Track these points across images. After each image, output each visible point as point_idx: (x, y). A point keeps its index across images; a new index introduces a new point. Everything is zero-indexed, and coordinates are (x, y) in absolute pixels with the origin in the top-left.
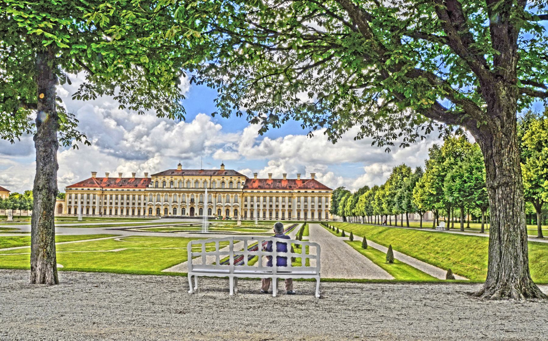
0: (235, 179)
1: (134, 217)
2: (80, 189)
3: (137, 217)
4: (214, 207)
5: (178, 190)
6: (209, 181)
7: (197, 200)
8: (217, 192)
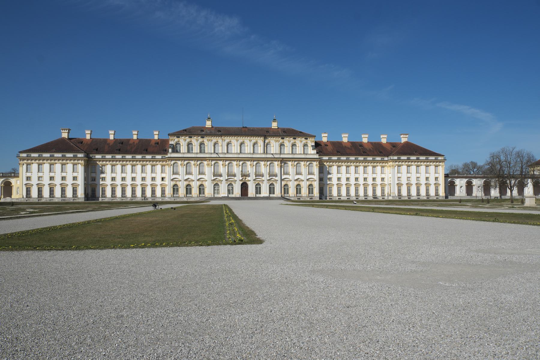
0: (300, 142)
5: (221, 156)
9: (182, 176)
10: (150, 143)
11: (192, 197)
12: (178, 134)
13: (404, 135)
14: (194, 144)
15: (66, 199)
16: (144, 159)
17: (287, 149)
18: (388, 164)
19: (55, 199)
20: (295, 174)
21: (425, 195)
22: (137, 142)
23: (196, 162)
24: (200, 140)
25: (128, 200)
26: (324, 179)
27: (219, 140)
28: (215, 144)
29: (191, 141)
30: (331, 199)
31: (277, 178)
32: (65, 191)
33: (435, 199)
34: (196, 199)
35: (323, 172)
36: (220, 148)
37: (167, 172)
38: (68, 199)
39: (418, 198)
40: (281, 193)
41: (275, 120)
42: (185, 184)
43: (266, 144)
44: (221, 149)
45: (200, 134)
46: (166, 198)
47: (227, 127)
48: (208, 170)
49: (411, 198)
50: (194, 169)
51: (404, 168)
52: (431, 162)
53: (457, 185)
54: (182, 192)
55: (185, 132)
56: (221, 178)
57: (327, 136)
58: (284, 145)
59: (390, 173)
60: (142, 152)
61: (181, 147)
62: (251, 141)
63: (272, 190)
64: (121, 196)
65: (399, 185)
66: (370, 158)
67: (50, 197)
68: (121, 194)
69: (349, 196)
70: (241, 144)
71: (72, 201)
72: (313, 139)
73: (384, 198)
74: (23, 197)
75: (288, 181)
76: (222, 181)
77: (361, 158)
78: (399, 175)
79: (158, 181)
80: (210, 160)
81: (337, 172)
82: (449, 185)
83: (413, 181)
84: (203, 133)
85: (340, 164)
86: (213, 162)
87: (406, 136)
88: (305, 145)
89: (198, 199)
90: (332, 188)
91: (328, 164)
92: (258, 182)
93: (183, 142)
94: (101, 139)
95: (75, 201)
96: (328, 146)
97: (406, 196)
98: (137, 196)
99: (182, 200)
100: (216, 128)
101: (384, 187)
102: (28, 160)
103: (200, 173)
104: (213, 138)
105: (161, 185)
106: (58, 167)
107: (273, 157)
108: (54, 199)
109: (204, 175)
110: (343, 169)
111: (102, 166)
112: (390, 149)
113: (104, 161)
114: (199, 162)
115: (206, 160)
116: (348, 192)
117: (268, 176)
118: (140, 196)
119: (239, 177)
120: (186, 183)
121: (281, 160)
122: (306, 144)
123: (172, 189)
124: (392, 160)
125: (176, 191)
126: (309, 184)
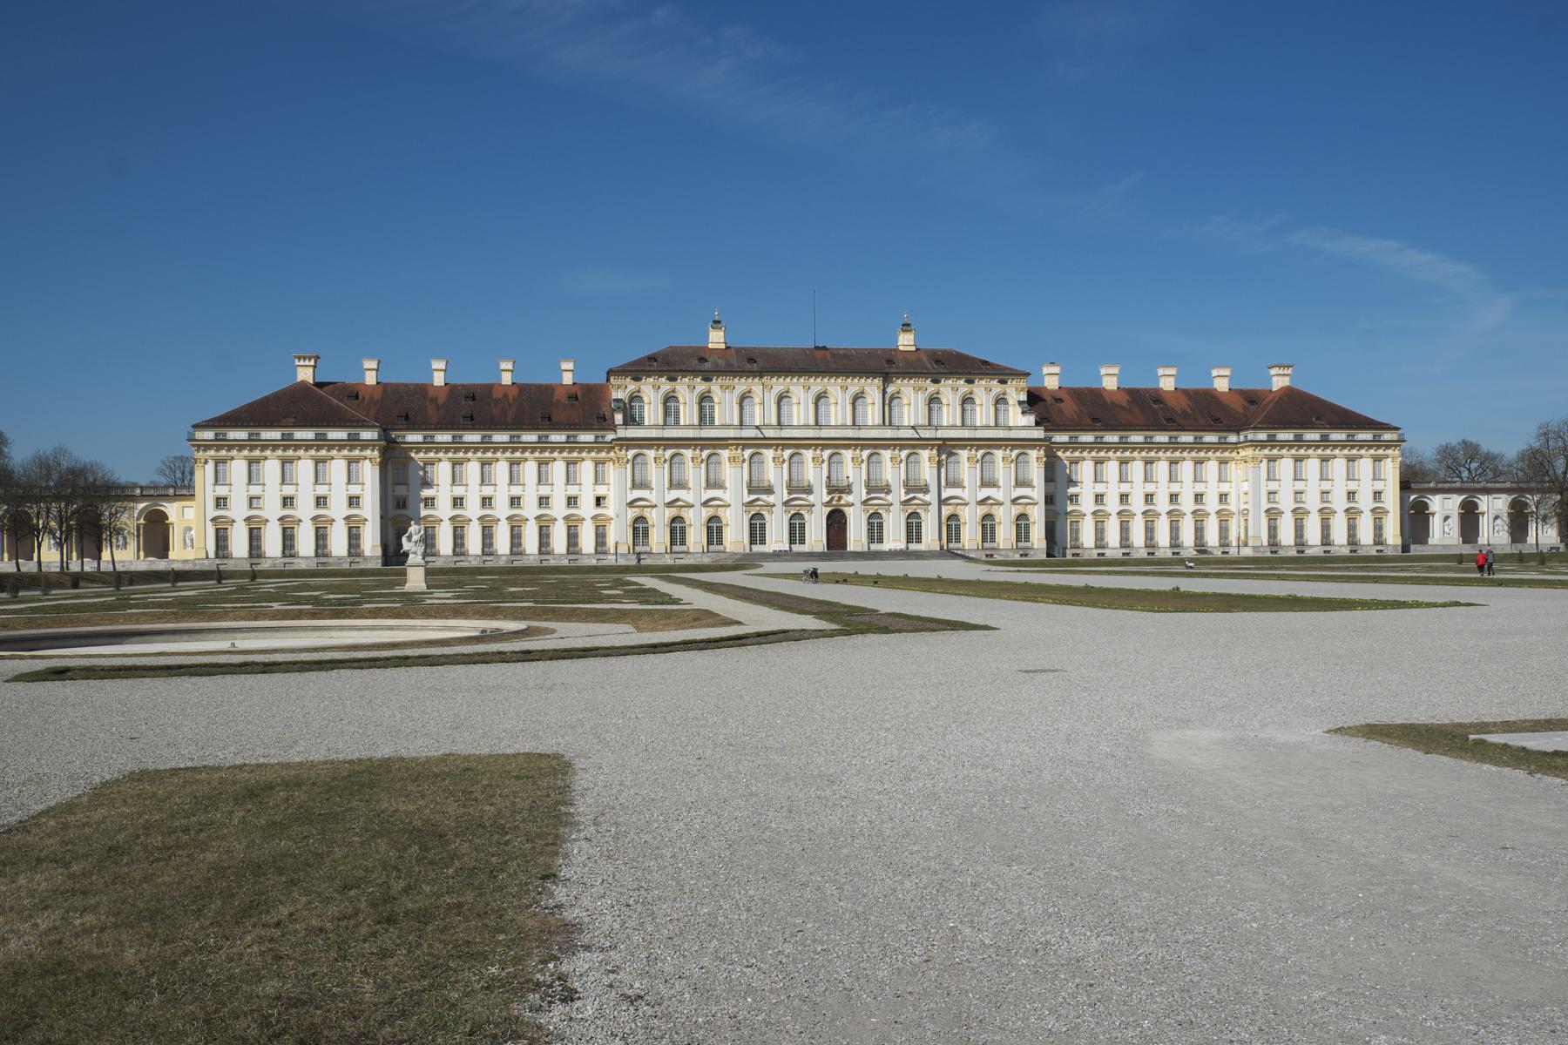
0: (985, 392)
1: (553, 562)
2: (273, 434)
3: (565, 562)
6: (878, 397)
9: (658, 492)
10: (553, 394)
11: (688, 553)
12: (637, 371)
13: (1280, 367)
14: (681, 400)
15: (330, 560)
16: (542, 446)
17: (949, 414)
18: (1238, 453)
19: (300, 561)
20: (979, 483)
21: (1345, 542)
22: (514, 392)
23: (698, 451)
24: (701, 386)
25: (502, 563)
26: (1058, 500)
27: (755, 386)
28: (743, 398)
29: (674, 391)
30: (1078, 555)
31: (927, 498)
32: (292, 537)
33: (1374, 553)
34: (700, 560)
35: (1057, 479)
36: (757, 409)
37: (612, 482)
38: (336, 559)
39: (1325, 552)
40: (940, 539)
41: (906, 327)
42: (667, 515)
43: (887, 397)
44: (762, 411)
45: (700, 371)
46: (609, 557)
47: (769, 349)
48: (732, 473)
49: (1307, 552)
50: (694, 473)
51: (1285, 466)
52: (1361, 447)
53: (1433, 514)
54: (658, 538)
55: (655, 364)
56: (771, 499)
57: (1058, 372)
58: (938, 401)
59: (1247, 481)
60: (538, 425)
61: (646, 407)
62: (847, 388)
63: (913, 530)
64: (480, 553)
65: (1273, 515)
66: (1187, 438)
67: (284, 556)
68: (480, 546)
69: (1129, 547)
70: (820, 397)
71: (346, 566)
72: (1023, 383)
73: (1227, 553)
74: (207, 558)
75: (958, 504)
76: (774, 505)
77: (1161, 437)
78: (1273, 486)
79: (587, 509)
80: (738, 445)
81: (1093, 479)
82: (1412, 512)
83: (1313, 503)
84: (707, 366)
85: (1102, 454)
86: (748, 453)
87: (1286, 372)
88: (1000, 401)
89: (706, 560)
90: (1080, 523)
91: (1068, 454)
92: (797, 508)
93: (651, 392)
94: (407, 386)
95: (355, 566)
96: (1063, 402)
97: (1291, 546)
98: (527, 553)
99: (659, 563)
100: (739, 350)
101: (1228, 520)
102: (219, 448)
103: (710, 485)
104: (736, 380)
105: (594, 518)
106: (304, 468)
107: (916, 436)
108: (295, 561)
109: (722, 491)
110: (1112, 468)
111: (425, 464)
112: (1240, 410)
113: (431, 451)
114: (706, 453)
115: (726, 447)
116: (1124, 535)
117: (903, 491)
118: (536, 551)
119: (820, 496)
120: (670, 513)
121: (939, 446)
122: (1002, 396)
123: (630, 531)
124: (1251, 441)
125: (641, 535)
126: (1018, 512)
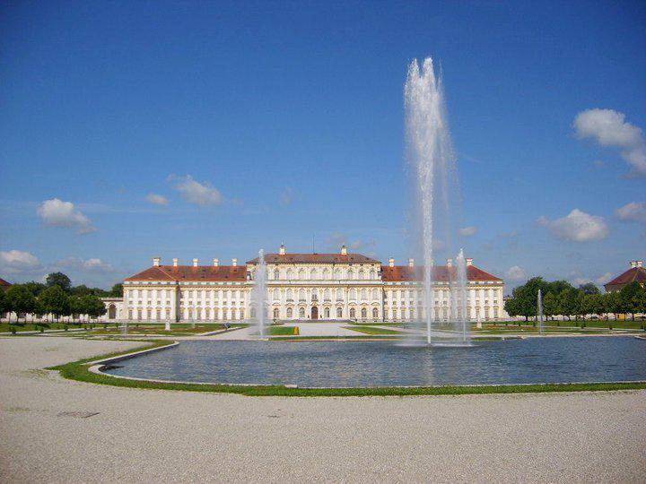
0: (367, 268)
2: (146, 282)
4: (346, 306)
7: (321, 297)
8: (349, 286)
24: (274, 267)
119: (309, 302)
